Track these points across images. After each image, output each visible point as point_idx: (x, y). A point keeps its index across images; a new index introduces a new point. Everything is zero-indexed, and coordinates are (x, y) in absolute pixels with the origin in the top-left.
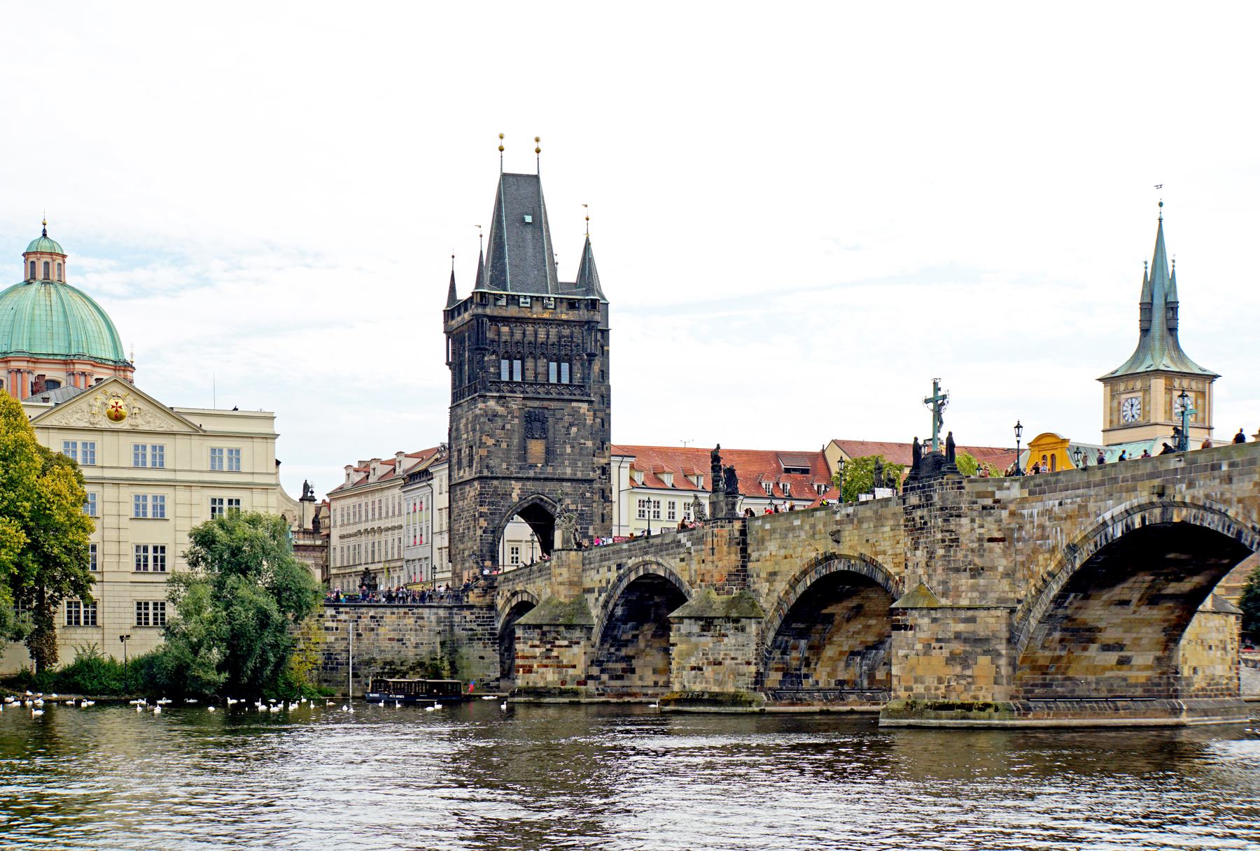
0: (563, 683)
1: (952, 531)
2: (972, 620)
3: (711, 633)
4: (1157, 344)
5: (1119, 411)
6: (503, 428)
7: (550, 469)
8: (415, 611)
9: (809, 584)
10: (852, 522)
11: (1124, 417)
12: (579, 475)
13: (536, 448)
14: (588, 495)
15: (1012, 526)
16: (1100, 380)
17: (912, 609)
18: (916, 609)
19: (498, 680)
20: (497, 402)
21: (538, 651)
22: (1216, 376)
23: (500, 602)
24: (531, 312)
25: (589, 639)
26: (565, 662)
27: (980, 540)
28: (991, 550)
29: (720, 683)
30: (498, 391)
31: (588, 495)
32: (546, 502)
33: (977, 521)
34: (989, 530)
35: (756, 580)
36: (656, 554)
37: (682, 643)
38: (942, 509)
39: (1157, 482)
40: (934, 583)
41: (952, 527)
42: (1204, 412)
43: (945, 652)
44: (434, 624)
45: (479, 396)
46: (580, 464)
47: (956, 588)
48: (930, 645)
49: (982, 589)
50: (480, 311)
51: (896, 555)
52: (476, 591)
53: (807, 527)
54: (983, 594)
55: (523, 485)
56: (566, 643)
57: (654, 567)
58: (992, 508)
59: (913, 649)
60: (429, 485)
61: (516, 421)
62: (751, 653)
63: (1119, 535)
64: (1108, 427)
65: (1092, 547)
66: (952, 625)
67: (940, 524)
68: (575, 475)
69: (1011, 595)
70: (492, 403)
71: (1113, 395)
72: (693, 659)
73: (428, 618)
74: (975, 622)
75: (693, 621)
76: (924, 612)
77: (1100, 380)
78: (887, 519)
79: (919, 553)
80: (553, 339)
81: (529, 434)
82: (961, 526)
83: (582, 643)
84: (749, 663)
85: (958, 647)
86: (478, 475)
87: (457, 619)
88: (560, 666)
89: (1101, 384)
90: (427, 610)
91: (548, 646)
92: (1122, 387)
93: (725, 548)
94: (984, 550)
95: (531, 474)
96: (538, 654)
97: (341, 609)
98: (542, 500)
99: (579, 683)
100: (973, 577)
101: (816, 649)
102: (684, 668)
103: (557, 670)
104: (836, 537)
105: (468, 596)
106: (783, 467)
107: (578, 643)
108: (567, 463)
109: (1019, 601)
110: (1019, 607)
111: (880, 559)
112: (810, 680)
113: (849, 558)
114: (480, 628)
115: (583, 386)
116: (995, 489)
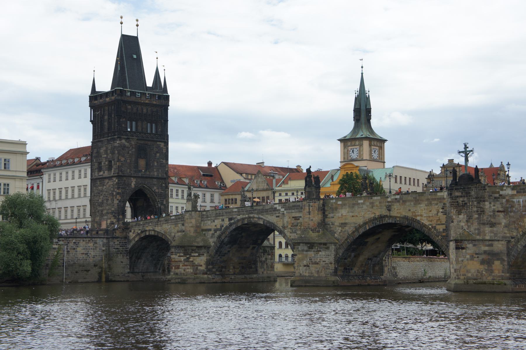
1: (481, 207)
2: (491, 245)
3: (313, 250)
4: (363, 126)
5: (348, 153)
6: (128, 153)
7: (148, 173)
8: (93, 239)
9: (368, 228)
10: (399, 202)
11: (350, 156)
12: (160, 176)
13: (142, 163)
14: (164, 185)
15: (508, 206)
16: (339, 140)
17: (465, 240)
18: (466, 240)
19: (129, 273)
20: (126, 141)
21: (182, 259)
22: (386, 140)
23: (132, 235)
24: (141, 99)
25: (208, 252)
26: (196, 263)
27: (494, 211)
28: (499, 216)
30: (126, 136)
31: (164, 185)
32: (146, 188)
33: (492, 203)
34: (497, 207)
35: (332, 226)
38: (476, 198)
40: (472, 229)
41: (481, 206)
42: (382, 155)
44: (101, 246)
45: (118, 138)
46: (160, 171)
48: (473, 256)
49: (495, 232)
50: (119, 98)
51: (429, 217)
52: (119, 230)
53: (368, 204)
55: (136, 180)
57: (256, 219)
58: (499, 198)
59: (465, 258)
60: (41, 178)
61: (134, 150)
62: (332, 259)
64: (343, 160)
67: (476, 204)
68: (158, 176)
69: (508, 235)
70: (123, 141)
72: (305, 262)
73: (99, 243)
74: (493, 246)
75: (304, 244)
76: (470, 242)
77: (339, 140)
78: (423, 201)
79: (461, 216)
82: (485, 205)
83: (205, 255)
84: (331, 263)
86: (116, 175)
87: (111, 243)
88: (193, 265)
90: (98, 239)
91: (188, 256)
92: (349, 144)
93: (316, 212)
94: (496, 216)
95: (140, 175)
96: (183, 260)
97: (60, 239)
98: (144, 187)
100: (491, 227)
101: (357, 256)
102: (300, 266)
104: (389, 209)
105: (116, 232)
106: (202, 173)
107: (203, 255)
108: (155, 170)
109: (512, 238)
110: (513, 240)
111: (418, 218)
112: (353, 271)
113: (396, 217)
114: (121, 248)
115: (162, 135)
116: (500, 190)
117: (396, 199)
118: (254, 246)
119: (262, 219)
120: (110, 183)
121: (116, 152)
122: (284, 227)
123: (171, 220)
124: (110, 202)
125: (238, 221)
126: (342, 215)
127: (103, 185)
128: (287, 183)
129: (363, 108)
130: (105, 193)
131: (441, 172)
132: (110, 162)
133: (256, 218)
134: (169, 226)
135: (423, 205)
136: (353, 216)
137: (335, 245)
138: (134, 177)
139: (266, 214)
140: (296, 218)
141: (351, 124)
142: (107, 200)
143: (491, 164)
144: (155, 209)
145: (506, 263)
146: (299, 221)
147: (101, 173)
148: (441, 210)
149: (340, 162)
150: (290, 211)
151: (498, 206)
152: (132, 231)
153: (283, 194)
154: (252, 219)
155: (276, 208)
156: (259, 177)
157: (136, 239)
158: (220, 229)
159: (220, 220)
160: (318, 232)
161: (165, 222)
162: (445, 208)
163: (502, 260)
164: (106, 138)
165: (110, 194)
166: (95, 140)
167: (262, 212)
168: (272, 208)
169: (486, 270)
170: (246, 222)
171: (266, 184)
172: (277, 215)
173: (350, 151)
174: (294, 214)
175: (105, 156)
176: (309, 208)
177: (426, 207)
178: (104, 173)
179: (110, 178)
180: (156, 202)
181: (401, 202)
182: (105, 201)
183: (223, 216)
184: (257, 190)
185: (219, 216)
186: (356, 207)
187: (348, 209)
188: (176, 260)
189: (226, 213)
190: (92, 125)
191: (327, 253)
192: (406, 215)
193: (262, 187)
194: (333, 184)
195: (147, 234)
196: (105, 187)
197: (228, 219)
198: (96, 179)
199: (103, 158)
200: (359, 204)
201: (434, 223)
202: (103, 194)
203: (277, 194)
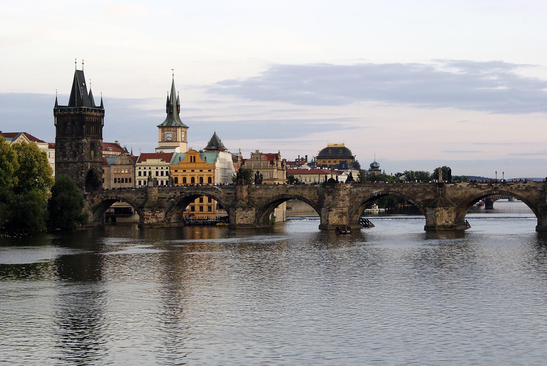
0: (158, 222)
2: (342, 209)
6: (87, 147)
7: (95, 159)
9: (274, 200)
10: (293, 188)
16: (157, 126)
21: (151, 214)
27: (344, 195)
28: (346, 197)
29: (247, 222)
32: (94, 169)
35: (253, 198)
36: (202, 190)
37: (238, 213)
39: (386, 187)
43: (338, 216)
47: (340, 204)
53: (276, 188)
54: (344, 205)
55: (91, 164)
56: (159, 212)
63: (376, 195)
64: (161, 141)
65: (369, 197)
66: (339, 210)
70: (85, 140)
71: (163, 131)
75: (241, 208)
77: (157, 126)
79: (330, 197)
80: (95, 121)
81: (91, 149)
83: (163, 212)
84: (253, 217)
85: (340, 214)
88: (157, 218)
91: (154, 213)
92: (166, 129)
93: (245, 191)
99: (162, 222)
103: (156, 219)
104: (287, 191)
107: (162, 212)
108: (98, 157)
109: (350, 206)
111: (304, 196)
113: (291, 195)
118: (184, 207)
119: (205, 193)
120: (75, 166)
122: (221, 198)
124: (75, 177)
125: (187, 193)
126: (259, 193)
129: (175, 105)
131: (251, 158)
132: (75, 152)
133: (201, 192)
134: (131, 195)
135: (307, 191)
136: (266, 194)
138: (90, 162)
139: (208, 191)
140: (229, 194)
141: (165, 115)
144: (97, 182)
145: (348, 217)
146: (231, 195)
147: (66, 159)
148: (316, 193)
149: (159, 142)
151: (345, 193)
152: (96, 196)
155: (215, 188)
156: (123, 156)
157: (100, 201)
159: (174, 193)
161: (126, 192)
163: (346, 216)
164: (71, 137)
169: (340, 220)
170: (193, 194)
171: (128, 161)
172: (215, 192)
173: (166, 135)
177: (308, 191)
178: (69, 159)
179: (74, 163)
180: (99, 177)
181: (295, 188)
183: (175, 190)
184: (121, 165)
186: (268, 190)
187: (263, 190)
188: (147, 215)
191: (251, 212)
192: (297, 194)
193: (125, 163)
194: (181, 163)
195: (110, 198)
196: (69, 168)
197: (179, 192)
198: (61, 162)
199: (67, 149)
201: (312, 199)
202: (68, 172)
203: (137, 168)
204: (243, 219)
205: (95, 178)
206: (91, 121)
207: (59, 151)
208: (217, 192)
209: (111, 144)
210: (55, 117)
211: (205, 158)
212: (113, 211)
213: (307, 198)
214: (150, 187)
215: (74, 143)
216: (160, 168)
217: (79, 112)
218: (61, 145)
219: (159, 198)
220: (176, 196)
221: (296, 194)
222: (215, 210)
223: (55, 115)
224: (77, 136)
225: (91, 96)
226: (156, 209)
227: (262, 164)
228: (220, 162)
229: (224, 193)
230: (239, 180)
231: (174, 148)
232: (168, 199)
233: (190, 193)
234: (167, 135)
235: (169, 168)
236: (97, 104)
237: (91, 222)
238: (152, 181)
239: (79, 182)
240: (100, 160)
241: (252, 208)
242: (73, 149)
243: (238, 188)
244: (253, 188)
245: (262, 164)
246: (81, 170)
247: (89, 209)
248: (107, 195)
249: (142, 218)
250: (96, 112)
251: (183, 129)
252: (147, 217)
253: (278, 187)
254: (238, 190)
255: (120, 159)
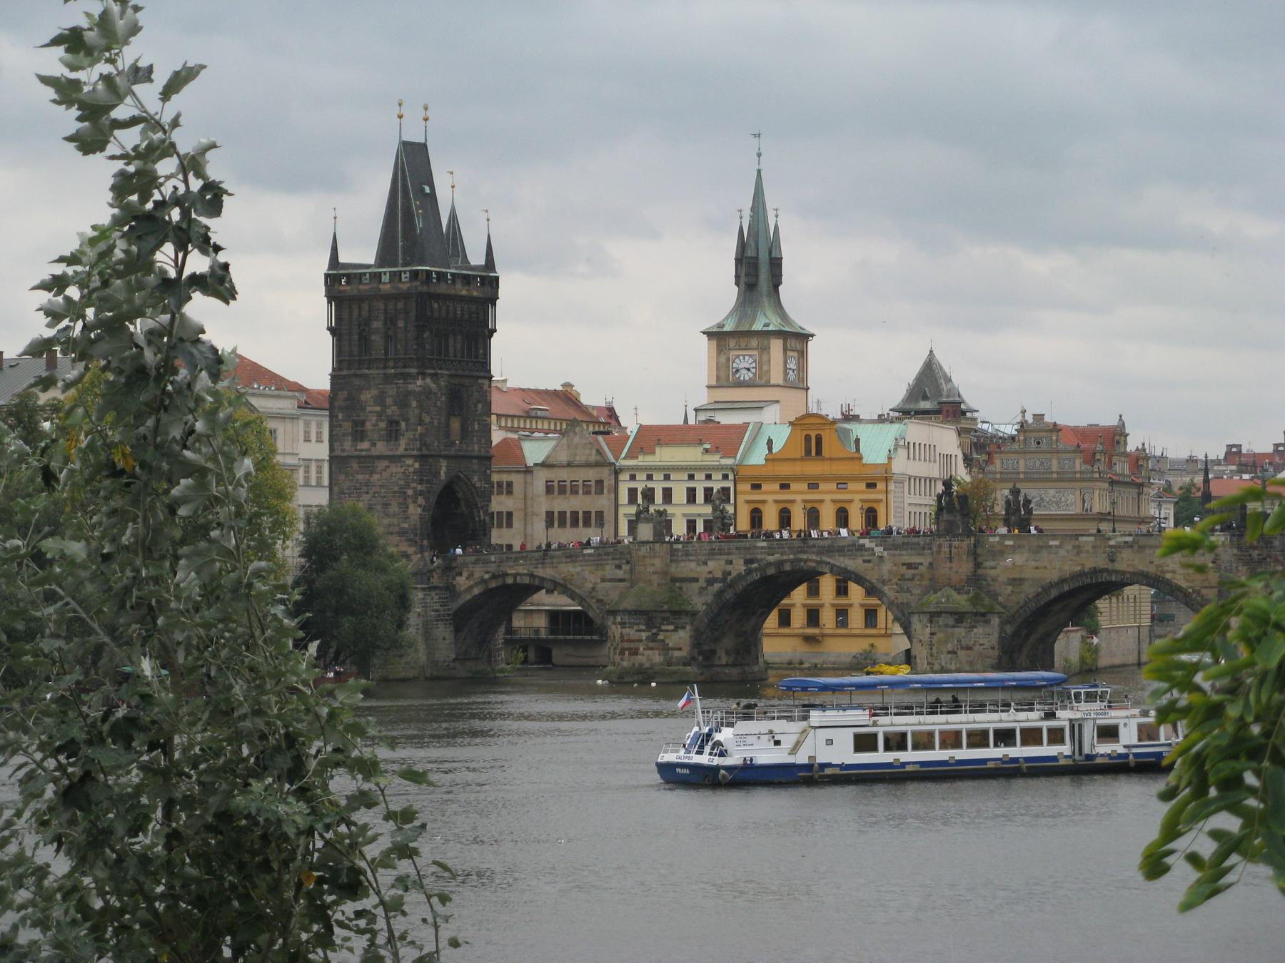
7: (465, 447)
9: (1066, 588)
10: (1131, 547)
21: (644, 635)
22: (812, 336)
23: (462, 582)
26: (671, 645)
36: (818, 553)
38: (1282, 551)
50: (425, 289)
53: (1070, 547)
61: (443, 398)
62: (994, 639)
64: (714, 383)
70: (428, 380)
71: (720, 350)
77: (704, 333)
81: (451, 413)
83: (688, 627)
84: (993, 648)
86: (415, 453)
88: (665, 648)
89: (705, 337)
91: (654, 631)
92: (732, 343)
93: (965, 557)
95: (453, 452)
99: (685, 664)
107: (684, 628)
111: (1168, 576)
113: (1124, 573)
117: (1125, 542)
119: (829, 563)
121: (414, 404)
122: (884, 582)
123: (584, 555)
124: (394, 508)
125: (770, 564)
127: (371, 474)
128: (654, 453)
129: (764, 256)
130: (374, 489)
132: (393, 423)
134: (579, 569)
136: (1037, 568)
137: (1000, 617)
138: (446, 457)
140: (909, 566)
142: (386, 505)
143: (931, 352)
146: (917, 571)
147: (365, 445)
149: (709, 387)
150: (897, 552)
152: (465, 574)
153: (641, 476)
154: (802, 564)
156: (575, 433)
157: (476, 591)
158: (723, 580)
159: (723, 562)
160: (968, 592)
162: (1218, 562)
164: (381, 371)
165: (395, 492)
166: (340, 369)
167: (828, 551)
168: (854, 545)
170: (787, 567)
171: (594, 452)
172: (867, 558)
173: (734, 362)
174: (905, 558)
175: (378, 409)
176: (950, 551)
178: (374, 445)
179: (392, 459)
181: (1136, 547)
182: (379, 507)
183: (729, 554)
184: (569, 465)
185: (721, 554)
186: (1044, 553)
187: (1026, 555)
189: (737, 549)
190: (330, 337)
191: (987, 630)
193: (584, 458)
195: (510, 581)
196: (376, 477)
198: (349, 457)
200: (1051, 547)
202: (371, 492)
203: (624, 477)
204: (955, 653)
205: (464, 508)
206: (451, 315)
207: (342, 420)
208: (869, 561)
209: (546, 392)
210: (329, 302)
211: (857, 441)
212: (541, 622)
213: (1179, 583)
214: (643, 542)
215: (392, 390)
216: (700, 476)
217: (409, 285)
218: (350, 398)
219: (674, 580)
220: (729, 573)
221: (1141, 567)
222: (890, 625)
223: (331, 296)
224: (405, 367)
225: (454, 233)
226: (664, 619)
227: (1055, 462)
228: (912, 457)
229: (895, 565)
230: (946, 516)
231: (758, 407)
232: (705, 585)
233: (780, 564)
234: (737, 361)
235: (731, 477)
236: (476, 257)
237: (445, 661)
238: (648, 520)
239: (406, 525)
240: (483, 450)
241: (990, 616)
242: (389, 412)
243: (940, 546)
244: (992, 546)
245: (1055, 462)
246: (415, 485)
247: (439, 616)
248: (502, 569)
249: (615, 649)
250: (468, 283)
251: (792, 343)
252: (632, 645)
253: (1077, 543)
254: (939, 552)
255: (565, 447)
